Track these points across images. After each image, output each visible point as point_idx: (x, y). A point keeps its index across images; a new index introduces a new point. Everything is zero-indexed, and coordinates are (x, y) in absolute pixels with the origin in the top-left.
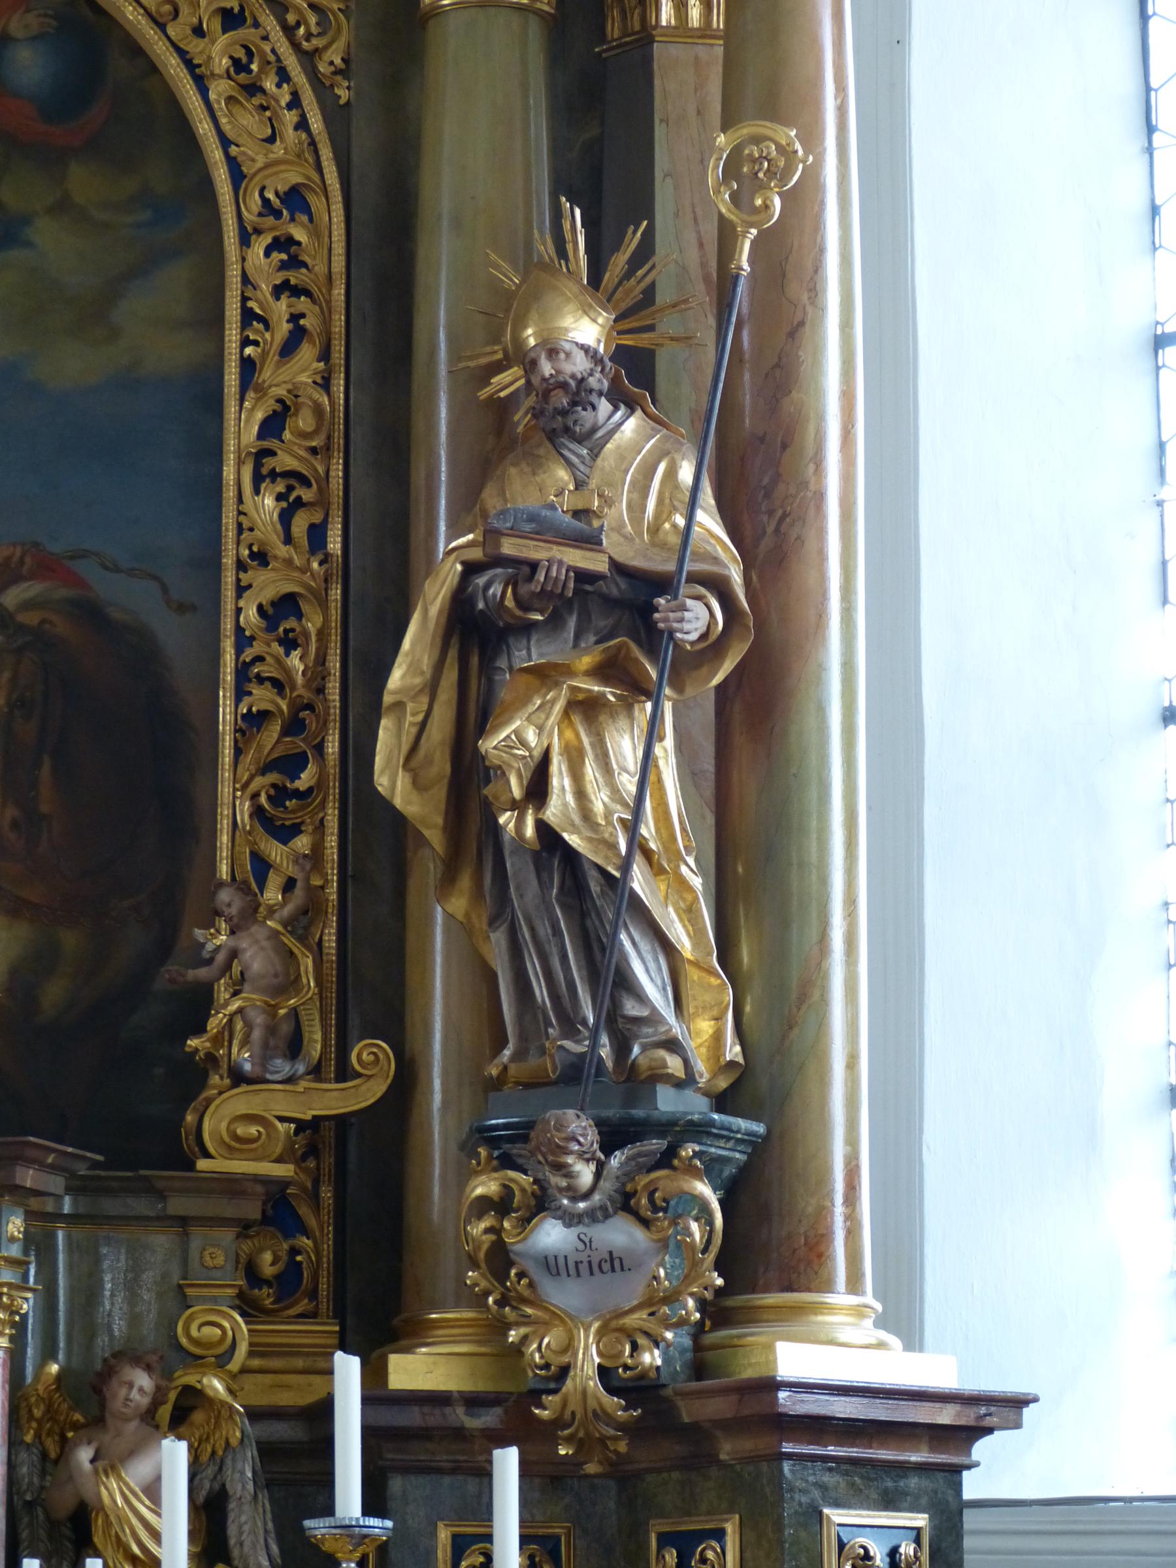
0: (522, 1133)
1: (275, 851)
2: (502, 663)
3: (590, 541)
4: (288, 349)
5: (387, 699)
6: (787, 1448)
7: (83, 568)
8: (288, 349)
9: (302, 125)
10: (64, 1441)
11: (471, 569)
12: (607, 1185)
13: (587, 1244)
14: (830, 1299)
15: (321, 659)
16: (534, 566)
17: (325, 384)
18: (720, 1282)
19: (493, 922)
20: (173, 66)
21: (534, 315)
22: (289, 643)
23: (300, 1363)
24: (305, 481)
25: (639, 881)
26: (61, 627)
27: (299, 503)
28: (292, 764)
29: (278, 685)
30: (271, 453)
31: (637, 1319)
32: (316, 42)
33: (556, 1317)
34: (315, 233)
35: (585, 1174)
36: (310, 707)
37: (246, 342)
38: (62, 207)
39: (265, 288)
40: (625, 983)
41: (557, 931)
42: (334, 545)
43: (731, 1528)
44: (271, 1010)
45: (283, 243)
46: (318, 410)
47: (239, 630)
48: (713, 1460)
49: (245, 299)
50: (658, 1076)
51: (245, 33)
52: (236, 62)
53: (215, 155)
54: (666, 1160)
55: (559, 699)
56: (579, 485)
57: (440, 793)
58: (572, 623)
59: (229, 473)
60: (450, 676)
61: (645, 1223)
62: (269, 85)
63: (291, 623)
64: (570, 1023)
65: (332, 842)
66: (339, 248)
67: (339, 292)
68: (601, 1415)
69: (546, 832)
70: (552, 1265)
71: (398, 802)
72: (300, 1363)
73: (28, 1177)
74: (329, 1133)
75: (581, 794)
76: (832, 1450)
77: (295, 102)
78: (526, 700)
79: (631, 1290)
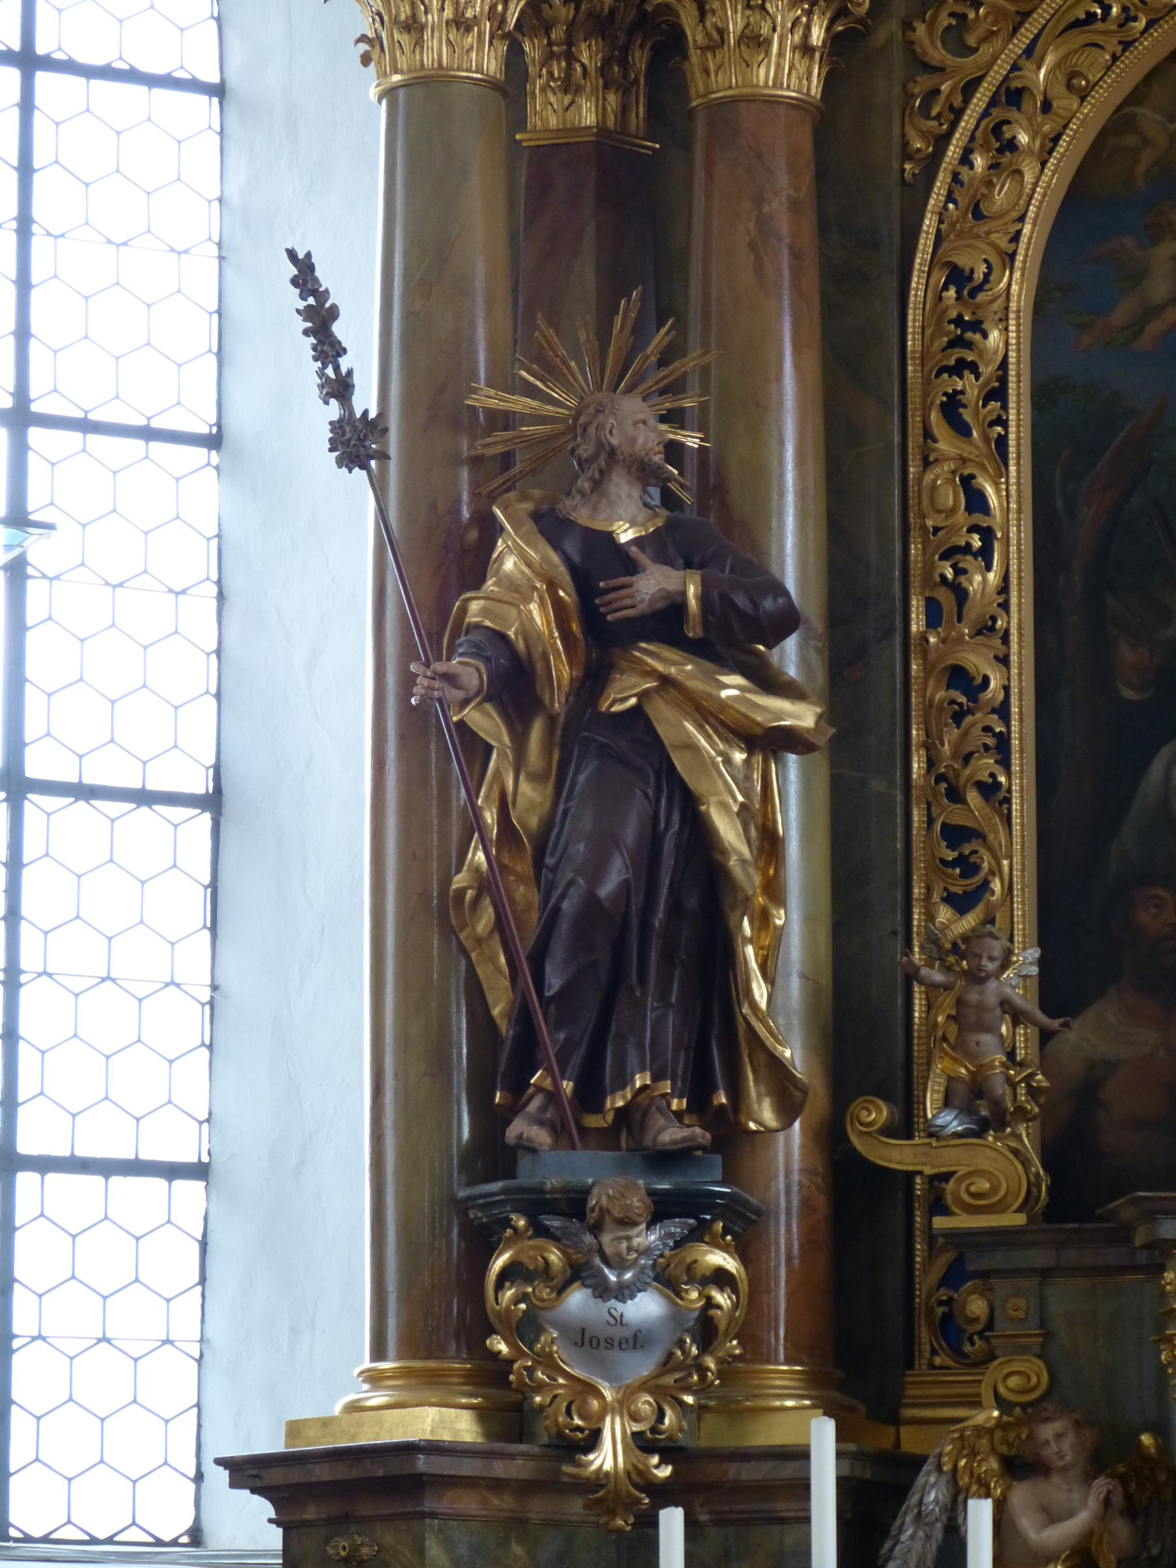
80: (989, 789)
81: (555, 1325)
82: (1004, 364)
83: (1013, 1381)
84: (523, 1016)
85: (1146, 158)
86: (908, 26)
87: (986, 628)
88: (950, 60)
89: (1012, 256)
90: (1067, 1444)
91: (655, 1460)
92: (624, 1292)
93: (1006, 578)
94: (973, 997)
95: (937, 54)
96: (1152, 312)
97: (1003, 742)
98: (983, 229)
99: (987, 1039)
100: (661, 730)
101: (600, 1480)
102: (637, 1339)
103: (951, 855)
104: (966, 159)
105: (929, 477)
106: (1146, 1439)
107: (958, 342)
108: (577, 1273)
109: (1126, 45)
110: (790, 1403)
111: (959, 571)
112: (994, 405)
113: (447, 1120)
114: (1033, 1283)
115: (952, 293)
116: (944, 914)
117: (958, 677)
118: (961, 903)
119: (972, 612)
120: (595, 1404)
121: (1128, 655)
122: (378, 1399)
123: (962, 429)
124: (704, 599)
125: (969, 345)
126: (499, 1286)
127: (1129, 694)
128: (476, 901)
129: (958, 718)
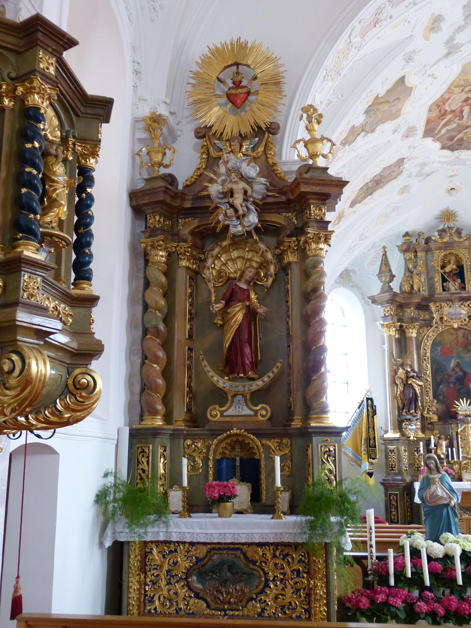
87: (428, 376)
95: (421, 332)
96: (438, 352)
102: (413, 429)
108: (410, 424)
117: (426, 379)
118: (427, 396)
121: (438, 378)
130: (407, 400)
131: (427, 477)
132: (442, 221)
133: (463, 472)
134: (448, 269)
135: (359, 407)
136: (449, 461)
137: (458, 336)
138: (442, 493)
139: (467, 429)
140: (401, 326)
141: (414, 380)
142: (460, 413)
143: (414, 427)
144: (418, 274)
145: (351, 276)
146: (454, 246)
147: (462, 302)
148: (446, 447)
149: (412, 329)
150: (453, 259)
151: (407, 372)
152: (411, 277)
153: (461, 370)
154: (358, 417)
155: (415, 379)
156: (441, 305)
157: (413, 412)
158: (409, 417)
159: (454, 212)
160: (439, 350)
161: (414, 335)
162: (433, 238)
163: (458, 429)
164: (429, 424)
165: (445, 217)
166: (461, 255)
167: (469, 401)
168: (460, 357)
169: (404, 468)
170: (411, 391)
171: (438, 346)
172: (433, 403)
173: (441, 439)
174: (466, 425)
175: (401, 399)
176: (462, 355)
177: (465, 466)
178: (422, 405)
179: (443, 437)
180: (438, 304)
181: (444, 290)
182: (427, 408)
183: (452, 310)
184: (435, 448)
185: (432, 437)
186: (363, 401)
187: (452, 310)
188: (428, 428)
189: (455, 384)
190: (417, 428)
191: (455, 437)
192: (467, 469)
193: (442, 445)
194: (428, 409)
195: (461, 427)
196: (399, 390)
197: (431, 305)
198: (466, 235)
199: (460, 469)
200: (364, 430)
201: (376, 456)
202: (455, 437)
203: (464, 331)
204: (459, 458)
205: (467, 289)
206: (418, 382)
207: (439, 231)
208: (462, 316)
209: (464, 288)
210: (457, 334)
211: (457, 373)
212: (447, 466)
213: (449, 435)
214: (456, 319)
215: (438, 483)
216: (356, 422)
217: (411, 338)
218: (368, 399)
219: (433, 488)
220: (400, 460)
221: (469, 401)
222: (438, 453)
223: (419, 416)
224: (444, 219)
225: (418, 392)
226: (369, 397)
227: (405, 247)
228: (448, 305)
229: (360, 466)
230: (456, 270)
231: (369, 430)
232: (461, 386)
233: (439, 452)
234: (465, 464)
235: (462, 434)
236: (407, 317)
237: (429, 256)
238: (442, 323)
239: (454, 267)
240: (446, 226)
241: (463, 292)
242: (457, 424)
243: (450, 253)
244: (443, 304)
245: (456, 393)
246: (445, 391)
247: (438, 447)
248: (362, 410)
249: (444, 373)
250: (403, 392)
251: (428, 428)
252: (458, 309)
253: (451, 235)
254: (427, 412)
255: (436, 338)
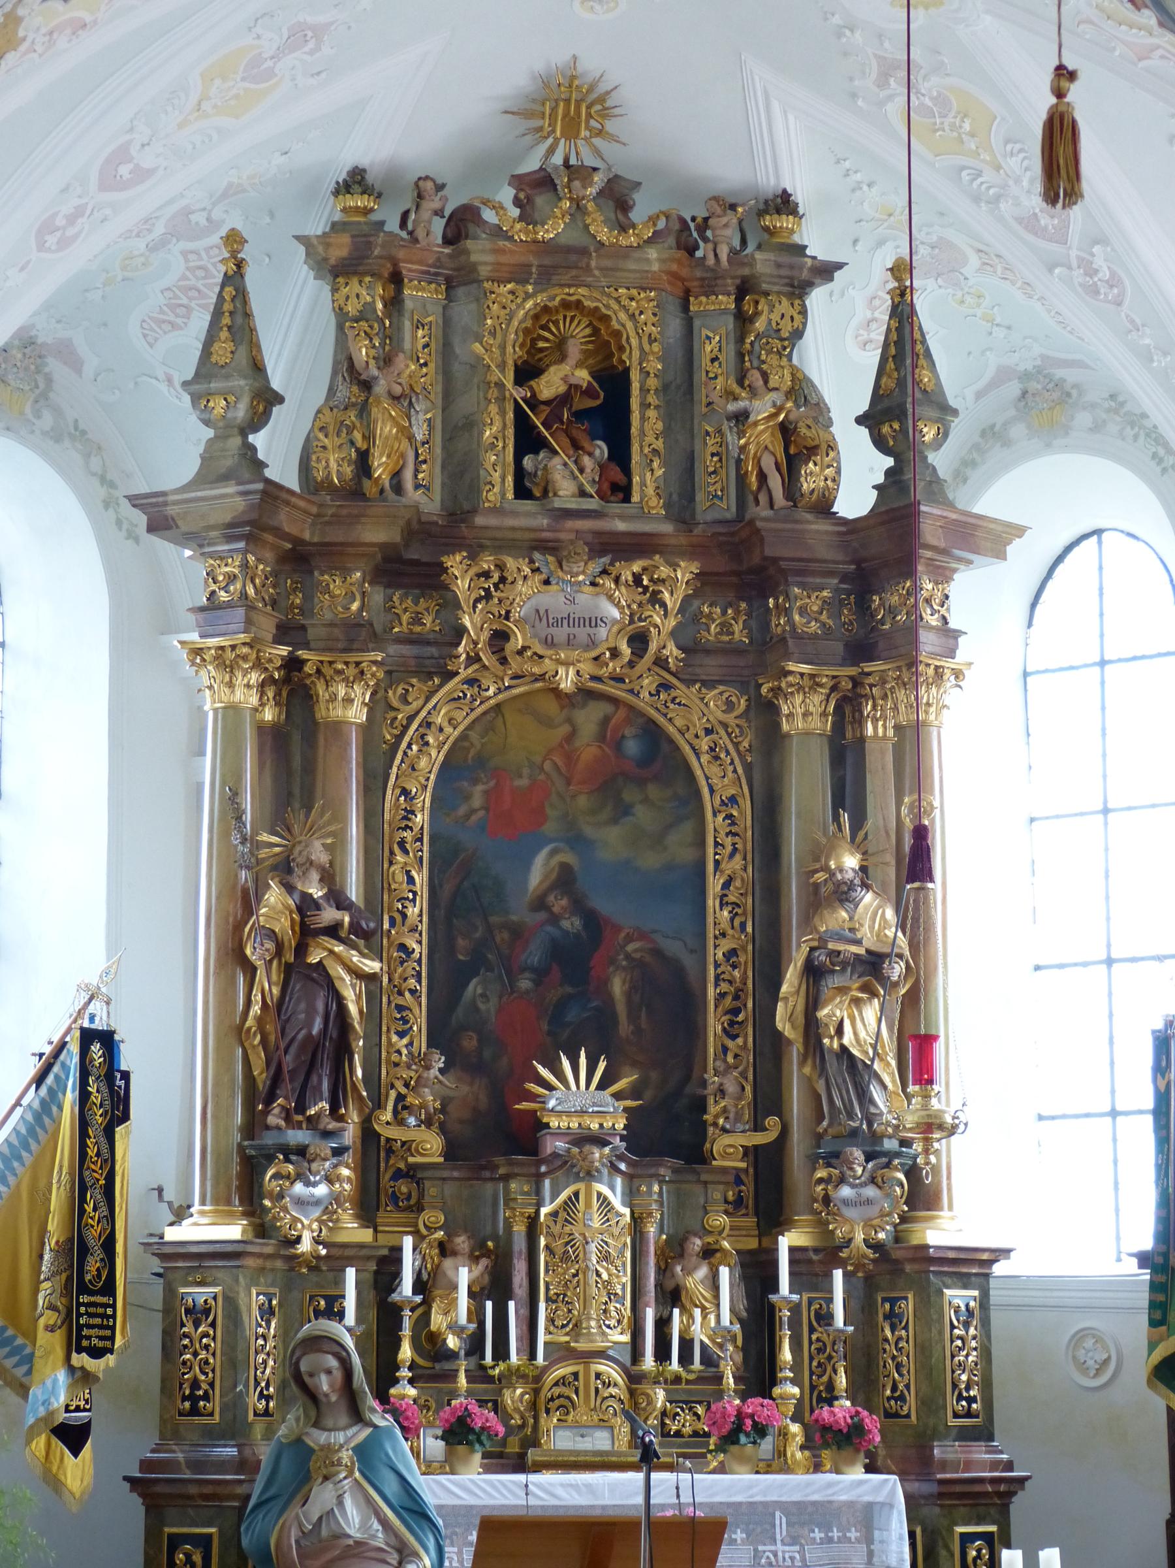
0: (837, 1155)
1: (730, 1044)
2: (823, 983)
3: (858, 942)
4: (732, 856)
5: (781, 995)
6: (932, 1269)
7: (653, 936)
8: (732, 856)
9: (735, 771)
10: (667, 1262)
11: (812, 949)
12: (867, 1175)
13: (859, 1195)
14: (941, 1213)
15: (745, 972)
16: (839, 953)
17: (745, 869)
18: (906, 1209)
19: (820, 1076)
20: (687, 749)
21: (833, 856)
22: (734, 967)
23: (744, 1233)
24: (739, 906)
25: (876, 1066)
26: (648, 959)
27: (737, 914)
28: (735, 1011)
29: (730, 982)
30: (726, 895)
31: (875, 1222)
32: (740, 739)
33: (846, 1220)
34: (740, 813)
35: (859, 1170)
36: (742, 990)
37: (716, 854)
38: (646, 801)
39: (722, 833)
40: (872, 1102)
41: (844, 1081)
42: (749, 929)
43: (910, 1296)
44: (736, 1106)
45: (729, 816)
46: (743, 880)
47: (715, 962)
48: (903, 1270)
49: (715, 837)
50: (883, 1136)
51: (714, 736)
52: (711, 748)
53: (703, 782)
54: (888, 1165)
55: (847, 999)
56: (851, 918)
57: (801, 1029)
58: (849, 970)
59: (710, 902)
60: (804, 987)
61: (880, 1187)
62: (722, 755)
63: (734, 959)
64: (851, 1115)
65: (750, 1040)
66: (749, 818)
67: (749, 833)
68: (864, 1256)
69: (844, 1049)
70: (846, 1202)
71: (786, 1034)
72: (744, 1233)
73: (662, 1171)
74: (752, 1150)
75: (855, 1034)
76: (946, 1269)
77: (732, 763)
78: (833, 999)
79: (873, 1211)
80: (413, 992)
81: (289, 1196)
82: (422, 828)
83: (432, 1219)
84: (276, 1080)
85: (472, 753)
86: (386, 691)
88: (402, 707)
89: (426, 787)
90: (466, 1244)
91: (321, 1247)
92: (315, 1184)
93: (421, 911)
94: (425, 1075)
95: (395, 703)
96: (473, 811)
97: (419, 974)
98: (417, 774)
99: (426, 1090)
100: (331, 972)
101: (303, 1254)
102: (317, 1202)
103: (398, 1016)
104: (409, 746)
105: (392, 869)
106: (490, 1244)
107: (405, 818)
108: (299, 1176)
109: (472, 710)
110: (350, 1225)
111: (404, 907)
112: (418, 844)
113: (231, 1114)
114: (439, 1183)
115: (402, 798)
116: (395, 1038)
117: (403, 947)
118: (401, 1035)
119: (409, 922)
120: (299, 1226)
121: (461, 942)
122: (206, 1220)
123: (406, 852)
124: (351, 924)
125: (409, 820)
126: (270, 1180)
127: (461, 957)
128: (255, 1033)
129: (402, 963)
130: (293, 1050)
131: (299, 1442)
132: (541, 129)
133: (549, 1422)
134: (550, 385)
135: (39, 1080)
136: (483, 1368)
137: (571, 737)
138: (364, 1527)
139: (581, 1206)
140: (293, 664)
141: (339, 948)
142: (554, 1123)
143: (322, 1190)
144: (396, 399)
145: (49, 380)
146: (588, 269)
147: (606, 560)
148: (471, 1294)
149: (349, 683)
150: (578, 333)
151: (306, 905)
152: (363, 410)
153: (579, 906)
154: (31, 1131)
155: (342, 941)
156: (501, 567)
157: (318, 1115)
158: (297, 1137)
159: (603, 88)
160: (477, 801)
161: (357, 714)
162: (489, 216)
163: (539, 1204)
164: (398, 1175)
165: (554, 110)
166: (623, 316)
167: (602, 1066)
168: (576, 840)
169: (254, 1402)
170: (320, 1006)
171: (475, 781)
172: (428, 1068)
173: (454, 1254)
174: (581, 1186)
175: (264, 1042)
176: (588, 831)
177: (557, 1391)
178: (372, 1078)
179: (462, 1242)
180: (487, 562)
181: (522, 492)
182: (393, 1094)
183: (554, 600)
184: (418, 1299)
185: (408, 1242)
186: (62, 1046)
187: (554, 600)
188: (394, 1198)
189: (540, 975)
190: (337, 1198)
191: (520, 1243)
192: (567, 1406)
193: (455, 1287)
194: (400, 1098)
195: (554, 1197)
196: (257, 997)
197: (455, 563)
198: (653, 219)
199: (534, 1406)
200: (58, 1199)
201: (112, 1338)
202: (520, 1243)
203: (607, 708)
204: (533, 1356)
205: (635, 498)
206: (356, 958)
207: (518, 181)
208: (602, 632)
209: (622, 491)
210: (569, 720)
211: (554, 919)
212: (470, 1393)
213: (495, 1237)
214: (570, 643)
215: (351, 1473)
216: (19, 1158)
217: (338, 728)
218: (88, 1037)
219: (322, 1497)
220: (235, 1361)
221: (602, 1066)
222: (433, 1327)
223: (350, 1134)
224: (552, 124)
225: (353, 1009)
226: (99, 1025)
227: (341, 249)
228: (536, 570)
229: (23, 1390)
230: (589, 392)
231: (83, 1200)
232: (569, 990)
233: (438, 1321)
234: (561, 1382)
235: (556, 1229)
236: (328, 616)
237: (464, 311)
238: (504, 661)
239: (583, 376)
240: (558, 159)
241: (616, 508)
242: (539, 1178)
243: (566, 305)
244: (511, 563)
245: (545, 1027)
246: (489, 1007)
247: (437, 1292)
248: (51, 1091)
249: (494, 919)
250: (278, 1009)
251: (394, 1198)
252: (585, 598)
253: (578, 205)
254: (395, 1112)
255: (463, 737)
